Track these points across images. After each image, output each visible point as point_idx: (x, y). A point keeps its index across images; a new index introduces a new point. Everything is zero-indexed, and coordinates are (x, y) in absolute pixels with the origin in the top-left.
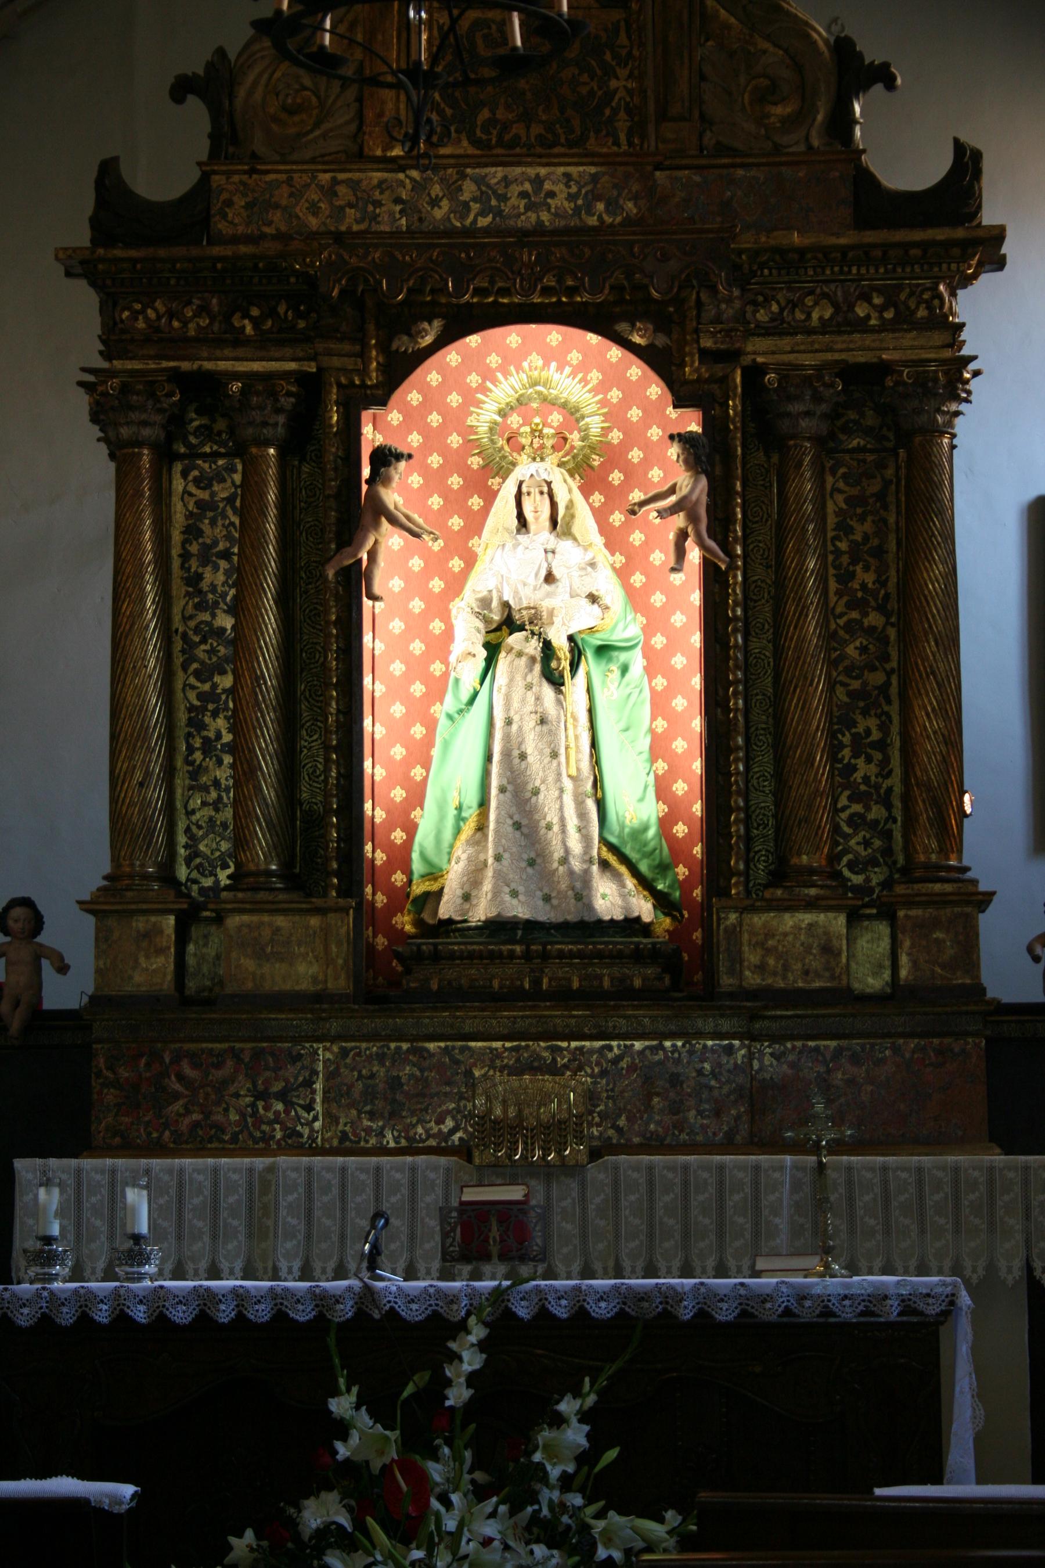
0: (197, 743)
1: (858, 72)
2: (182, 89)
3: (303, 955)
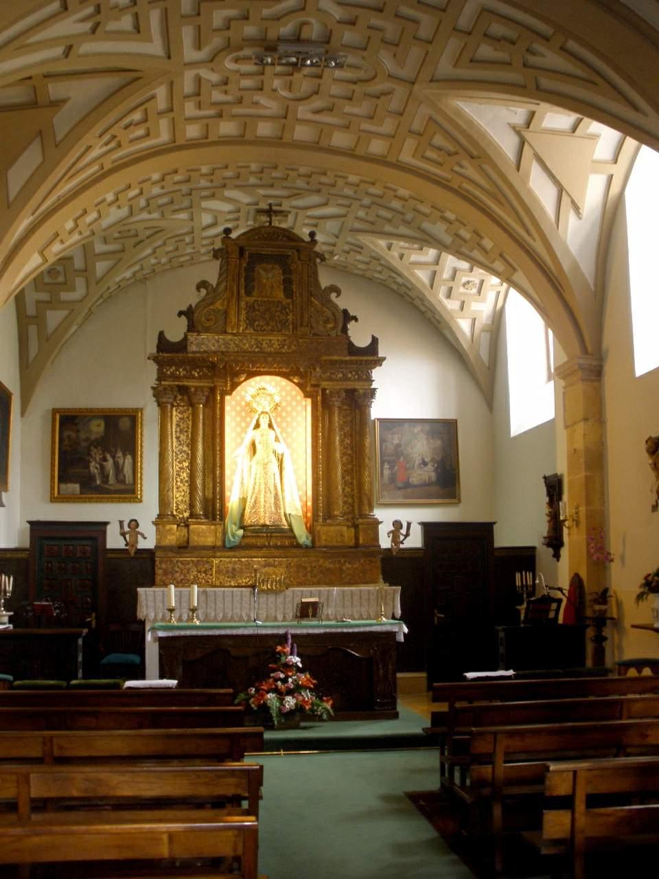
0: (179, 480)
1: (347, 317)
2: (180, 314)
3: (204, 533)
